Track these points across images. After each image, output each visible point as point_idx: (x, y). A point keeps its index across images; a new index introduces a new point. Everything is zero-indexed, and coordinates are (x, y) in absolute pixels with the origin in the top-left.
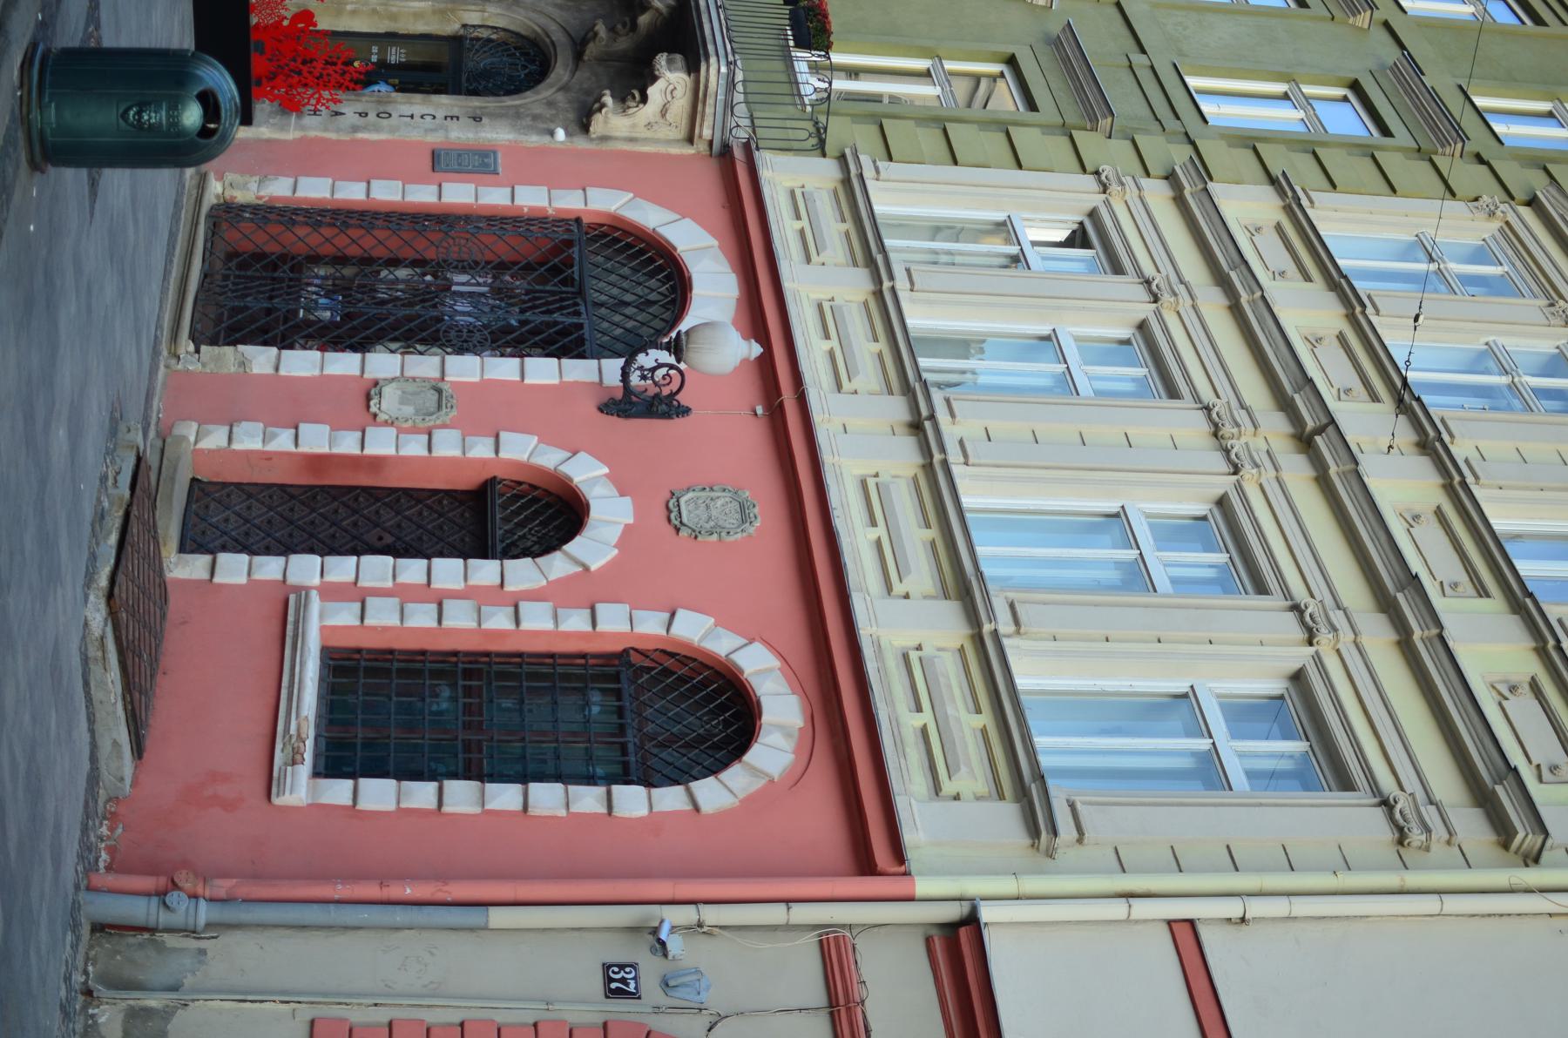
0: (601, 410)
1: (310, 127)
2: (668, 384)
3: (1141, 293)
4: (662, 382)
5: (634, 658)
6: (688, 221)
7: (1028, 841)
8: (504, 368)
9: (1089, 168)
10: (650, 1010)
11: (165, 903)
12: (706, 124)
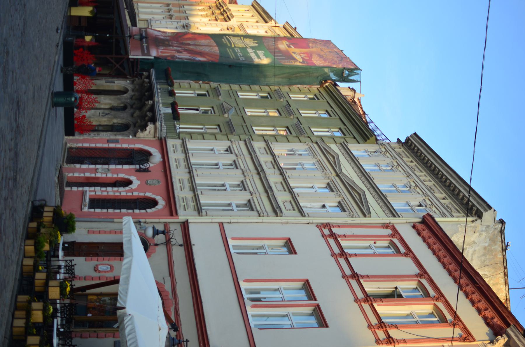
1: (85, 136)
3: (235, 156)
9: (229, 139)
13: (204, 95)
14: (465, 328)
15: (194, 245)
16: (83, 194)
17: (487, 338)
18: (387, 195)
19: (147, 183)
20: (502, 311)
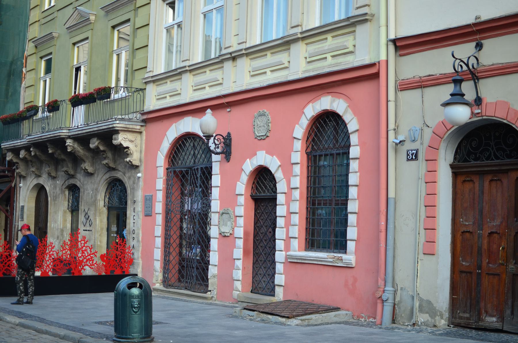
1: (138, 256)
2: (220, 139)
4: (220, 141)
5: (309, 150)
6: (167, 133)
7: (369, 23)
8: (215, 193)
10: (422, 146)
11: (386, 301)
12: (135, 128)
13: (49, 63)
19: (264, 138)
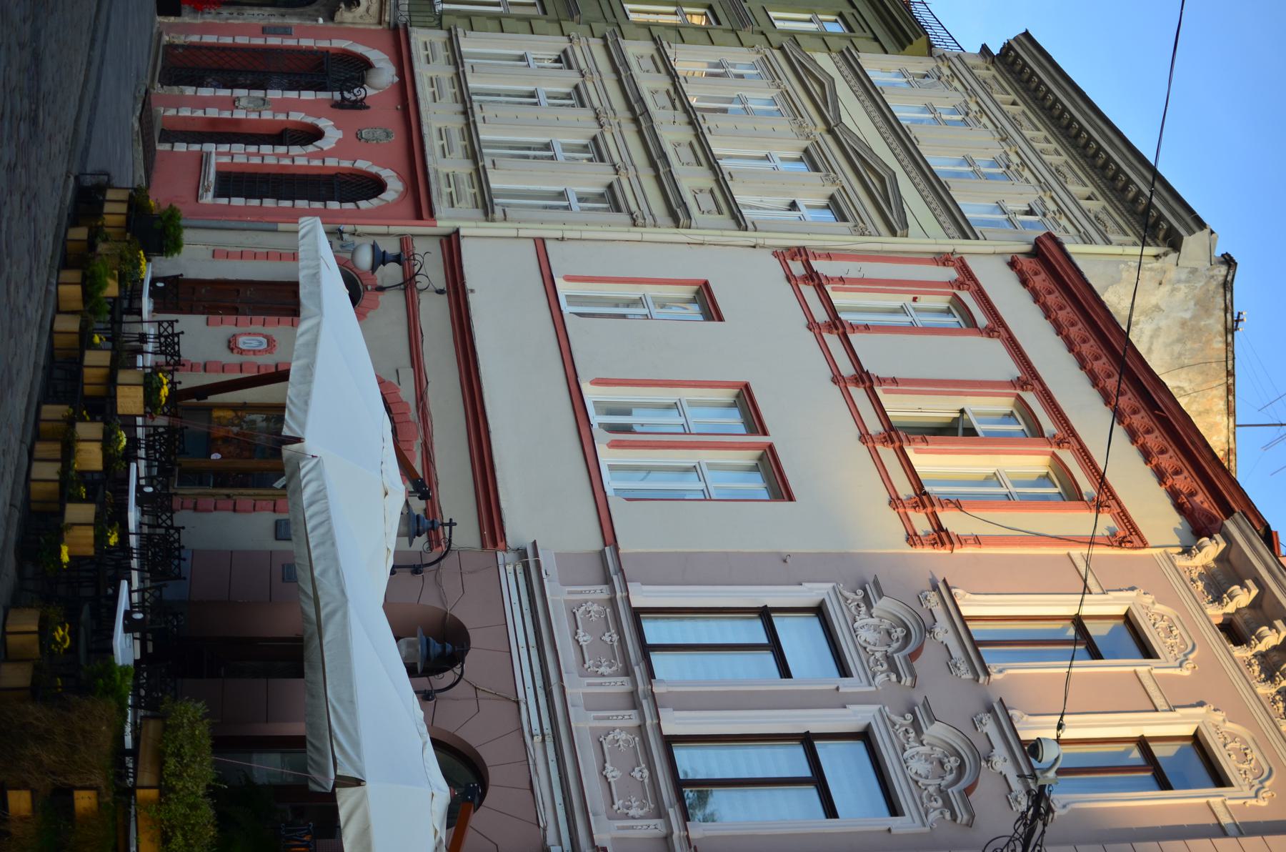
0: (332, 106)
1: (209, 18)
9: (566, 33)
14: (1124, 515)
15: (472, 291)
16: (202, 160)
17: (1177, 541)
18: (949, 183)
19: (359, 137)
20: (1215, 479)
